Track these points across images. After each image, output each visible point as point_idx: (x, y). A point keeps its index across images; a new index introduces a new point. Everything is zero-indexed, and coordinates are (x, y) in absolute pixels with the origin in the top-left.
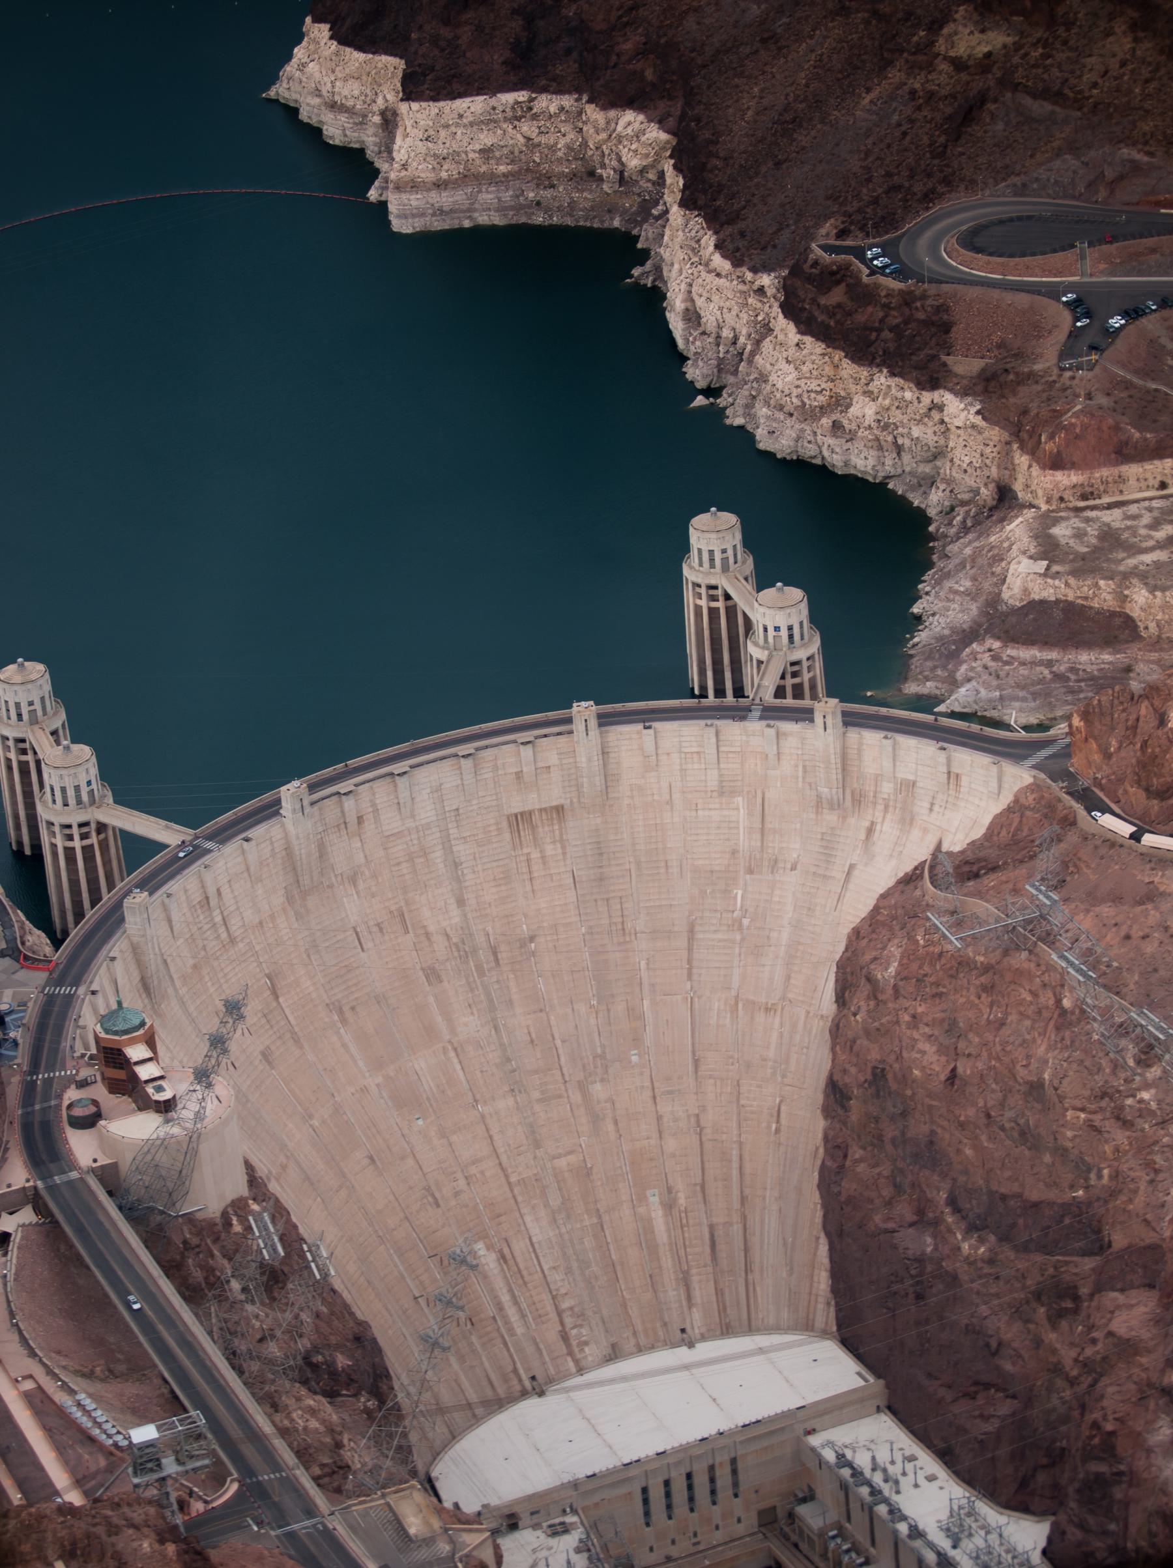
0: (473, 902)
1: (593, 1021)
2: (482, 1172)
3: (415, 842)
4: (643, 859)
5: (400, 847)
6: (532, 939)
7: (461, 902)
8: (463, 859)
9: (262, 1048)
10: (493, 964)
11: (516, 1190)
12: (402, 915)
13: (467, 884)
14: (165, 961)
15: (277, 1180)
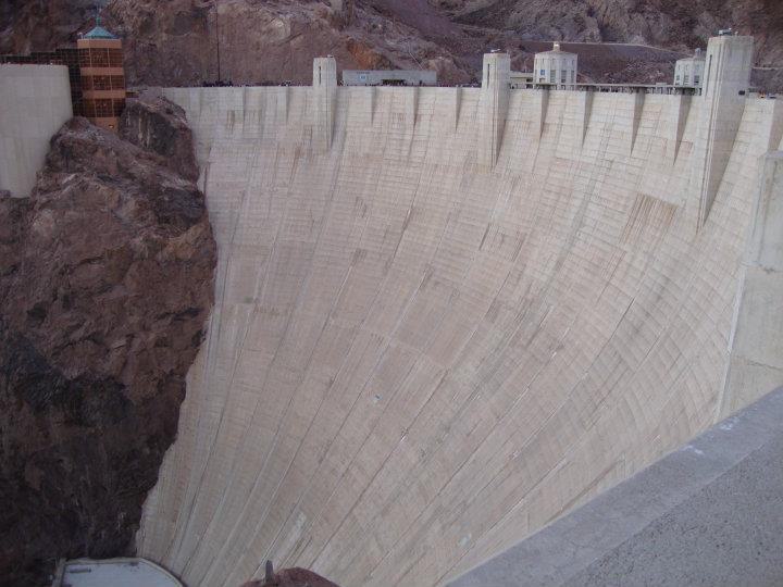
0: (565, 272)
1: (498, 470)
2: (355, 480)
3: (571, 178)
4: (672, 336)
5: (559, 176)
6: (561, 347)
7: (559, 264)
8: (587, 223)
9: (362, 247)
10: (524, 343)
11: (348, 521)
12: (522, 242)
13: (575, 250)
14: (346, 133)
15: (256, 310)
